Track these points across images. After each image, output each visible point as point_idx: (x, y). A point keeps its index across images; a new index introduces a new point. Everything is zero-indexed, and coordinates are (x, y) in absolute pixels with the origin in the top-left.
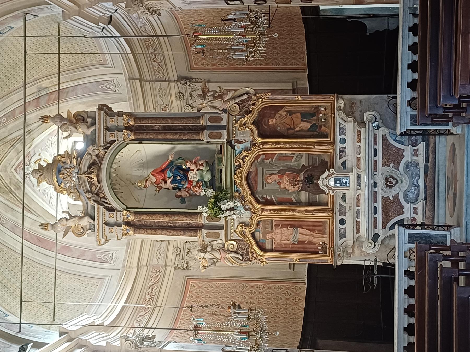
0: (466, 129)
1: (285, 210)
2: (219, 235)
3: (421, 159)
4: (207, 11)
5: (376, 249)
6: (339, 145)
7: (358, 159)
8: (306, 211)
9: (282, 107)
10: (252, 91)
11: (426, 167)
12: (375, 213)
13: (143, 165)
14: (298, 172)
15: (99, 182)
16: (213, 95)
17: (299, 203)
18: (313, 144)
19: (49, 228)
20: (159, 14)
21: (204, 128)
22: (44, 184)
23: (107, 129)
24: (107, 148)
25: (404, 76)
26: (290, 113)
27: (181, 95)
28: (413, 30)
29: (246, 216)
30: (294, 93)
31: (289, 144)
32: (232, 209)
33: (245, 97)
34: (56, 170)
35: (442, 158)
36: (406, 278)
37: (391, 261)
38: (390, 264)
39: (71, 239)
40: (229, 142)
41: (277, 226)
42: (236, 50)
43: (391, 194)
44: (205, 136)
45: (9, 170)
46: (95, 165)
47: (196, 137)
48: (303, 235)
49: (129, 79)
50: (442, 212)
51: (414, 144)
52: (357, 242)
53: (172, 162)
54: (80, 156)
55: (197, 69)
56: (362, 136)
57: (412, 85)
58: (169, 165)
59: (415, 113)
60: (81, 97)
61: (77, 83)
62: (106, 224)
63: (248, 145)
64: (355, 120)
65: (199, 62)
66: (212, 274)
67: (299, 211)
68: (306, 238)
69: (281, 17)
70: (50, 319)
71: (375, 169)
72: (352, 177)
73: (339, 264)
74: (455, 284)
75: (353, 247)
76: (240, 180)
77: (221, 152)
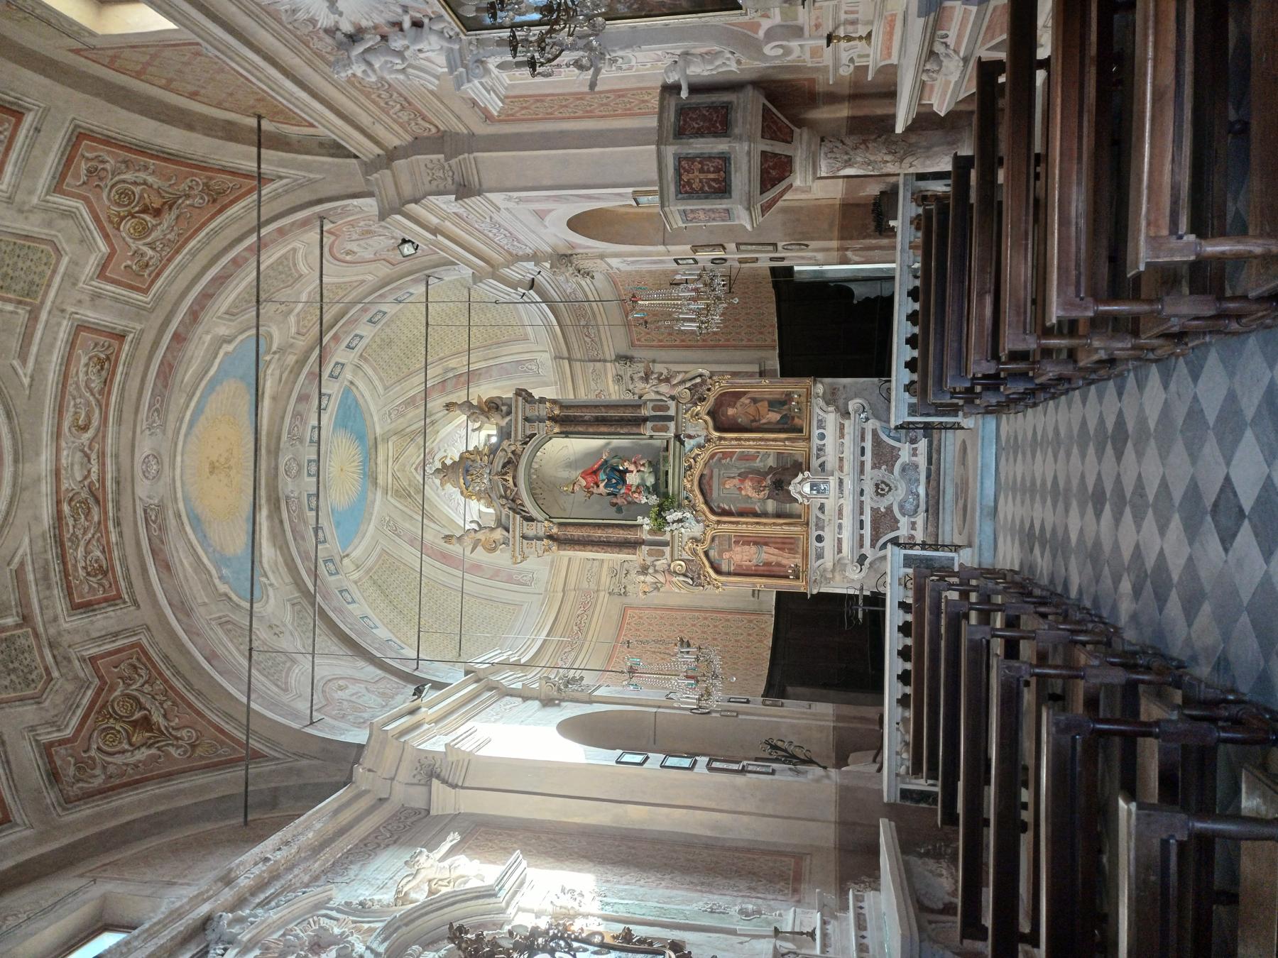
0: (980, 422)
1: (747, 523)
2: (663, 554)
3: (922, 460)
4: (650, 272)
5: (863, 574)
6: (816, 442)
7: (841, 459)
8: (774, 524)
9: (745, 393)
10: (706, 373)
11: (929, 470)
12: (862, 528)
13: (571, 465)
14: (765, 475)
15: (515, 485)
16: (658, 378)
17: (765, 514)
18: (784, 440)
19: (454, 541)
20: (593, 277)
21: (645, 420)
22: (449, 487)
23: (526, 419)
24: (526, 443)
25: (901, 353)
26: (755, 401)
27: (619, 378)
28: (913, 294)
29: (696, 529)
31: (754, 440)
32: (680, 521)
33: (698, 380)
34: (463, 469)
35: (949, 459)
36: (901, 612)
37: (881, 590)
38: (879, 593)
39: (481, 555)
40: (677, 437)
41: (737, 542)
42: (685, 320)
43: (882, 505)
44: (647, 430)
45: (407, 468)
46: (511, 464)
47: (635, 430)
48: (769, 555)
49: (556, 358)
50: (948, 528)
51: (913, 441)
52: (839, 565)
53: (606, 461)
54: (493, 451)
56: (846, 430)
57: (911, 365)
58: (602, 465)
59: (914, 400)
60: (496, 381)
61: (491, 362)
62: (524, 537)
63: (701, 440)
64: (837, 409)
66: (656, 602)
67: (765, 524)
68: (773, 559)
70: (455, 653)
71: (862, 472)
72: (833, 482)
73: (815, 592)
74: (964, 623)
75: (833, 571)
76: (690, 485)
77: (667, 449)
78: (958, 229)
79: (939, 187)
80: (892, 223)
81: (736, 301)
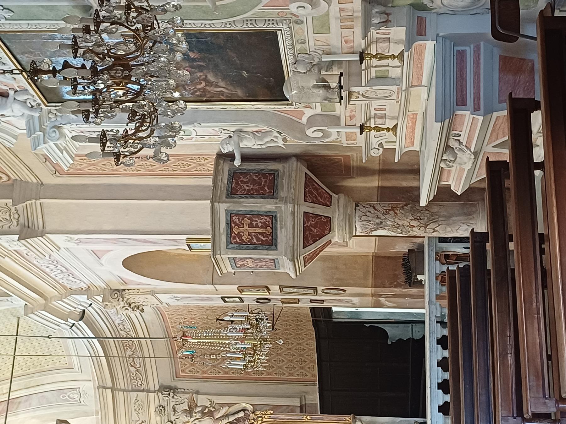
30: (301, 411)
55: (184, 377)
65: (187, 368)
69: (286, 319)
78: (479, 288)
79: (459, 249)
80: (420, 277)
81: (281, 342)
